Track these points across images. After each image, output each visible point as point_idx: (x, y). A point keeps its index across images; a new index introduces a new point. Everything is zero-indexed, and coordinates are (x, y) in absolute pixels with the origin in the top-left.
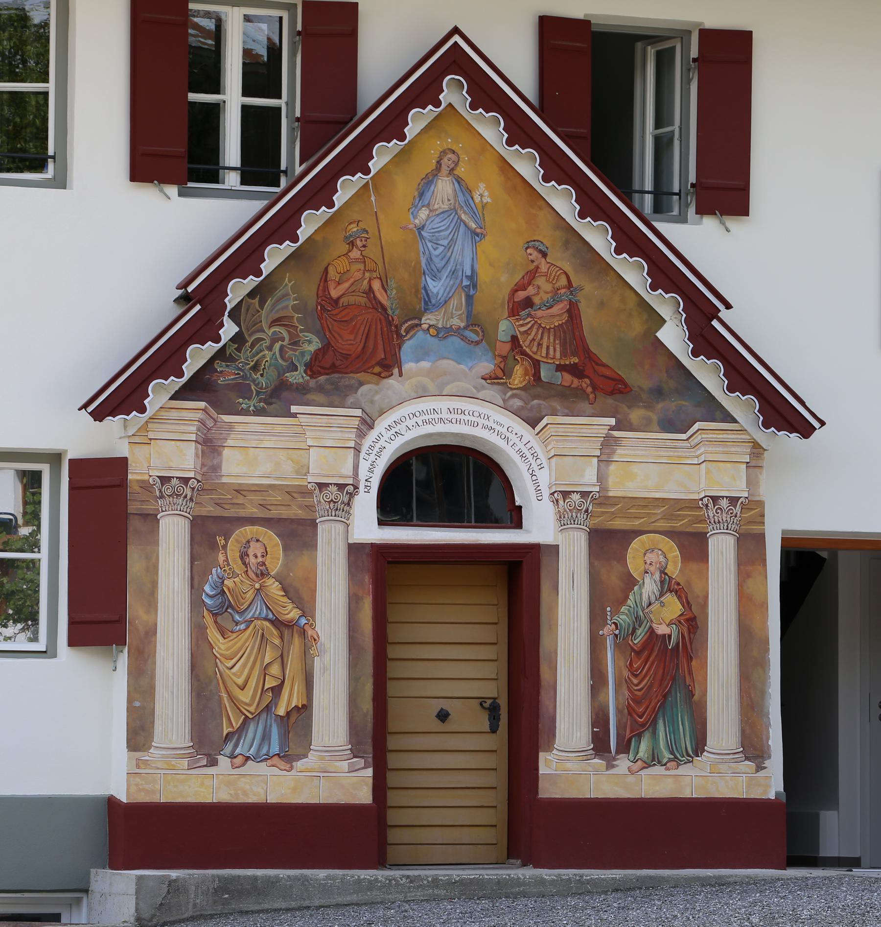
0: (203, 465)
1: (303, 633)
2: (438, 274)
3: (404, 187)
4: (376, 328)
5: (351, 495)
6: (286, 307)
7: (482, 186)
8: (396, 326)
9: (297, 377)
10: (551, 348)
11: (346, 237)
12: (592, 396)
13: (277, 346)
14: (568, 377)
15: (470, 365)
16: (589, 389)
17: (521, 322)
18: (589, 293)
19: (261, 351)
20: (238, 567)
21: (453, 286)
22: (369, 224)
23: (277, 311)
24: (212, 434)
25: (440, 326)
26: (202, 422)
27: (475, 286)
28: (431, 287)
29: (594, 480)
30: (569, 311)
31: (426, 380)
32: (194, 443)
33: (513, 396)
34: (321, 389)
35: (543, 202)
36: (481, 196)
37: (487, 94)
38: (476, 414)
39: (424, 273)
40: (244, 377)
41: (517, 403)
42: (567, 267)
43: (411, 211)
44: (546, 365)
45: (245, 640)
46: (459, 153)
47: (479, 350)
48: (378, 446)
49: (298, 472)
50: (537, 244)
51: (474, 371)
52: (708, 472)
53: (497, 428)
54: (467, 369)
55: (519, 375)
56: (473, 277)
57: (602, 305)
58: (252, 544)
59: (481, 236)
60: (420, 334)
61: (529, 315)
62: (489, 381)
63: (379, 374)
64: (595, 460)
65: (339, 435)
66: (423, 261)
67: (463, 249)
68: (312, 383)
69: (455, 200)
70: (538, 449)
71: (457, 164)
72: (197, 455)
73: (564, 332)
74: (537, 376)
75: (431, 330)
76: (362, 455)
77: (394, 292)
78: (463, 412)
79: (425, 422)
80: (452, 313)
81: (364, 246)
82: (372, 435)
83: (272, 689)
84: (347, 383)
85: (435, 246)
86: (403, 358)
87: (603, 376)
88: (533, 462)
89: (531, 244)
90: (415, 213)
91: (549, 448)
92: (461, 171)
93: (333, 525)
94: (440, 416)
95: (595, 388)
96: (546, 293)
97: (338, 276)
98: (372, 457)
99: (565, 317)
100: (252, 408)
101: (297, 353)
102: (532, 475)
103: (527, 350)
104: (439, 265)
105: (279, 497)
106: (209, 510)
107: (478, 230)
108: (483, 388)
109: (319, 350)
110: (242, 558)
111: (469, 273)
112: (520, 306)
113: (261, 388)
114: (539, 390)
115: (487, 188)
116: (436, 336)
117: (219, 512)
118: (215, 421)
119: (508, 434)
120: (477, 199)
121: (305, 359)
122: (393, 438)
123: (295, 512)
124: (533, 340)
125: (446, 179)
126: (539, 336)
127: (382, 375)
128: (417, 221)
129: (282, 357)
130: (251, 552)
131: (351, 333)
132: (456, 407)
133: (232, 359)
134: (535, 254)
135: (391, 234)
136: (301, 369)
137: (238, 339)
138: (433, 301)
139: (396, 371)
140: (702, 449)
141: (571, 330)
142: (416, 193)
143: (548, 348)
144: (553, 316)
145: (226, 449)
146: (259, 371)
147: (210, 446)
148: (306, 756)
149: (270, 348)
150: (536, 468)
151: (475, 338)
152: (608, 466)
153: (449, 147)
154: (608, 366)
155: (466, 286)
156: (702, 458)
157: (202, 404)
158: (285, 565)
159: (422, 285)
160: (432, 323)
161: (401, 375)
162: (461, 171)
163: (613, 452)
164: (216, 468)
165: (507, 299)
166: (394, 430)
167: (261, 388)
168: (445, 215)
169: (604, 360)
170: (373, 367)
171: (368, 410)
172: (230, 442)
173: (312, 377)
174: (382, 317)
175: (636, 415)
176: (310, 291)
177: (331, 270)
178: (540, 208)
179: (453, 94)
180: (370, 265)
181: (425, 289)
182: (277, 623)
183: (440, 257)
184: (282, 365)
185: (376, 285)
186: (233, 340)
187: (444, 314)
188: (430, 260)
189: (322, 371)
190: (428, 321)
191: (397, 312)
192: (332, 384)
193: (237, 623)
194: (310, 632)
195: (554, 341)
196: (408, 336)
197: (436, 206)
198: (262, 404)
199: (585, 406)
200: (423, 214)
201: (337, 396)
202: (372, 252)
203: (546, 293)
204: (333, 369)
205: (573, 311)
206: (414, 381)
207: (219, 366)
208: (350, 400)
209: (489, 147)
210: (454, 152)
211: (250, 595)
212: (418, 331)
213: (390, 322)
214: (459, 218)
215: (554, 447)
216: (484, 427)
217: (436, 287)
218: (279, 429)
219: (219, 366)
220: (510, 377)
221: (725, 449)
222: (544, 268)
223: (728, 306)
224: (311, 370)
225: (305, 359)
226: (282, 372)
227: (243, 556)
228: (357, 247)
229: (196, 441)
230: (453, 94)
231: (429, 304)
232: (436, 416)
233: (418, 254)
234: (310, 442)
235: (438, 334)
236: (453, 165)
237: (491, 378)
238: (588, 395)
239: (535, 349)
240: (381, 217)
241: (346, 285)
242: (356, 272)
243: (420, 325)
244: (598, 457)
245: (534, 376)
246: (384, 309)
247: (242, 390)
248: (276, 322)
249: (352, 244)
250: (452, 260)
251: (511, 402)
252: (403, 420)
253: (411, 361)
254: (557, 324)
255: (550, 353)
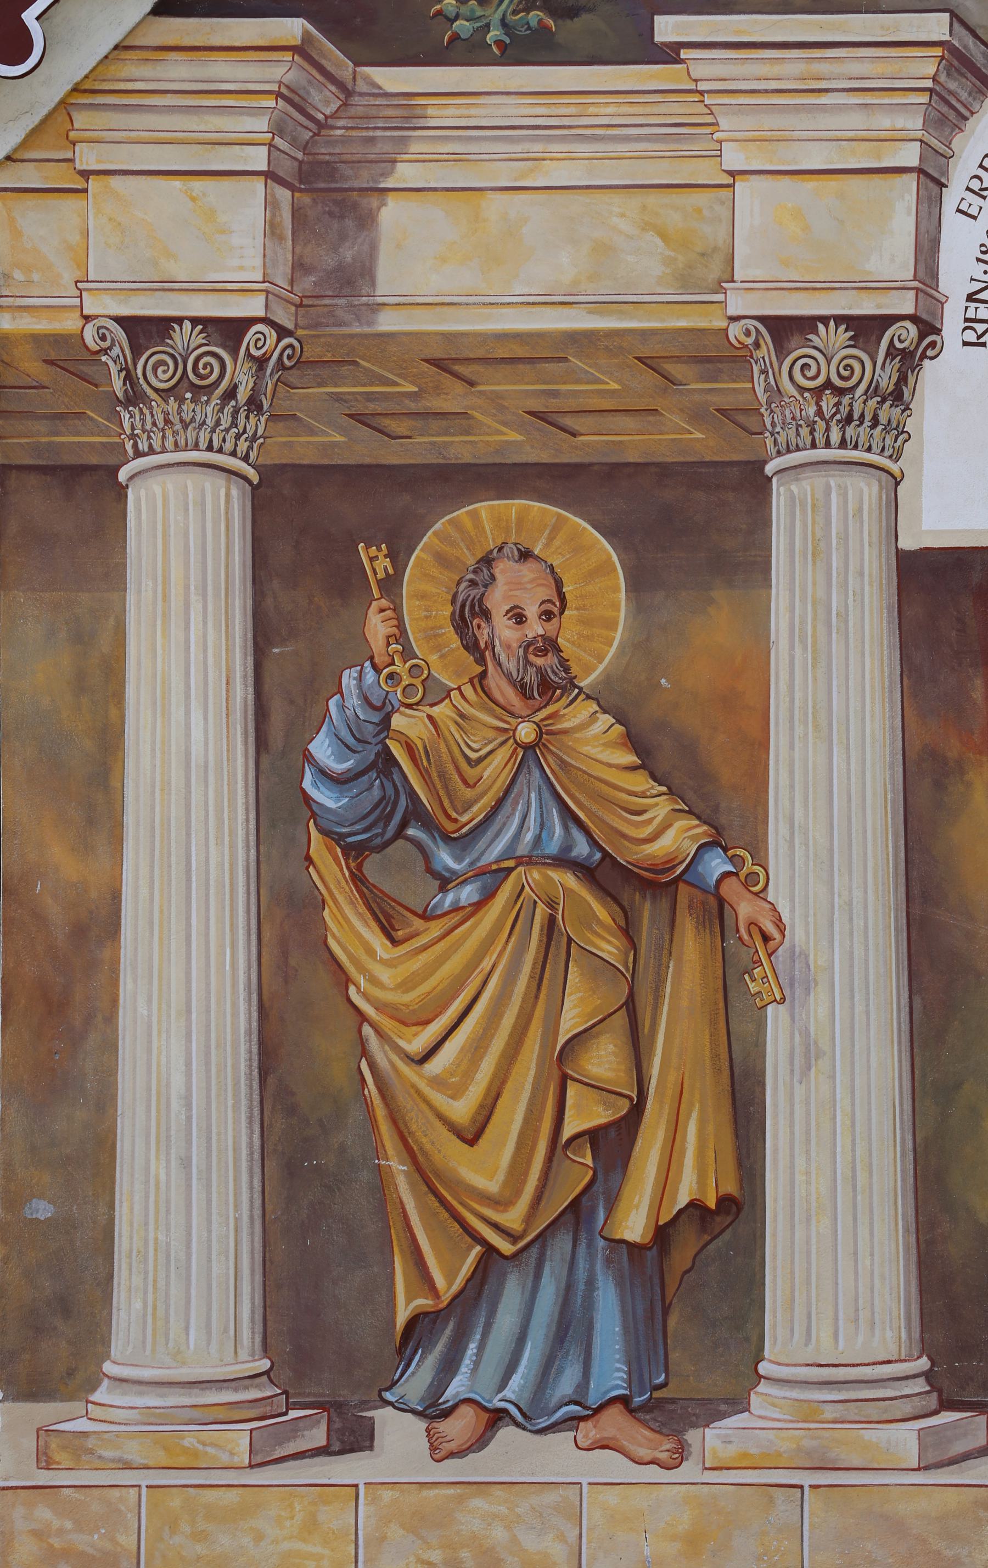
0: (299, 267)
1: (716, 912)
20: (445, 660)
24: (331, 142)
26: (290, 97)
32: (259, 184)
45: (478, 947)
49: (685, 281)
58: (504, 569)
65: (855, 122)
72: (272, 229)
76: (953, 196)
83: (594, 1136)
93: (834, 480)
100: (494, 34)
105: (608, 382)
106: (326, 440)
110: (461, 624)
117: (365, 449)
118: (347, 92)
123: (679, 436)
130: (498, 601)
145: (391, 199)
147: (325, 191)
148: (739, 1404)
157: (293, 28)
158: (640, 646)
164: (354, 279)
172: (406, 174)
182: (609, 875)
193: (445, 882)
194: (745, 909)
198: (535, 16)
211: (496, 770)
218: (607, 111)
227: (469, 616)
229: (269, 175)
234: (734, 158)
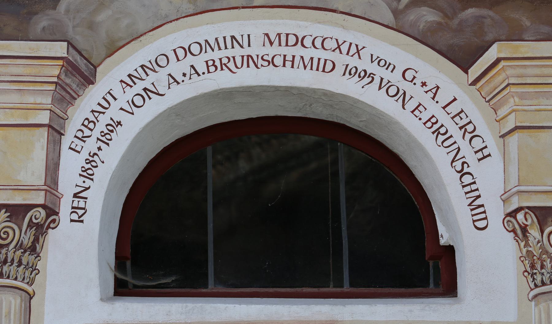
5: (40, 230)
38: (330, 44)
41: (427, 16)
48: (104, 120)
53: (380, 72)
65: (15, 98)
70: (477, 114)
76: (67, 140)
78: (300, 41)
79: (212, 66)
82: (92, 97)
88: (463, 144)
91: (502, 112)
94: (246, 51)
98: (91, 145)
102: (462, 173)
119: (404, 86)
122: (138, 101)
132: (284, 31)
166: (139, 87)
171: (81, 43)
208: (42, 22)
216: (349, 71)
232: (237, 52)
251: (412, 16)
252: (162, 61)
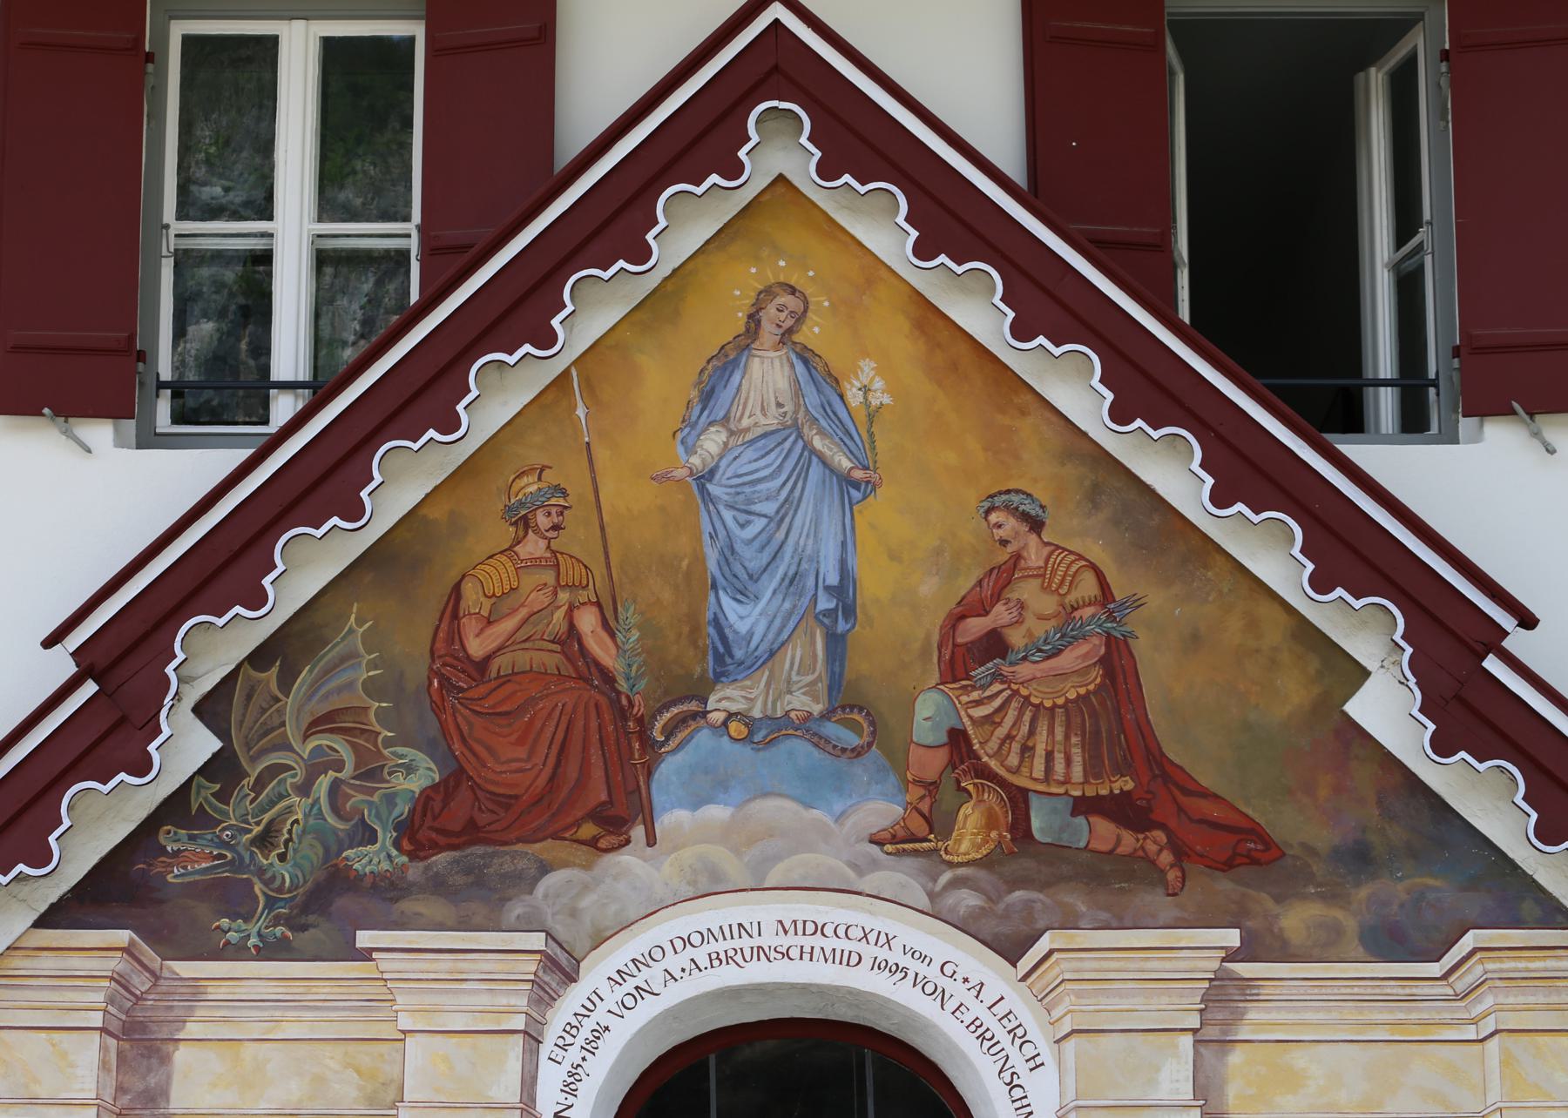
0: (120, 1089)
2: (751, 587)
3: (662, 380)
4: (586, 728)
6: (350, 685)
7: (867, 367)
8: (640, 721)
9: (375, 858)
10: (1059, 758)
11: (508, 509)
12: (1172, 875)
13: (323, 783)
14: (1105, 831)
15: (838, 807)
16: (1166, 858)
17: (975, 695)
18: (1158, 611)
19: (281, 797)
21: (790, 614)
22: (572, 475)
23: (326, 696)
24: (146, 1009)
25: (757, 713)
26: (120, 980)
27: (849, 611)
28: (732, 617)
29: (1186, 1091)
30: (1105, 662)
31: (719, 854)
32: (96, 1035)
33: (956, 883)
34: (438, 886)
35: (1029, 397)
36: (866, 390)
37: (862, 137)
38: (856, 933)
39: (714, 586)
40: (237, 865)
41: (968, 900)
42: (1097, 552)
43: (679, 436)
44: (1045, 800)
46: (808, 292)
47: (860, 771)
48: (588, 1024)
49: (371, 1100)
50: (1015, 498)
51: (849, 823)
52: (1507, 1061)
53: (914, 966)
54: (829, 820)
55: (971, 830)
56: (844, 590)
57: (1194, 641)
59: (870, 487)
60: (704, 738)
61: (997, 676)
62: (889, 848)
63: (593, 843)
64: (1187, 1041)
65: (484, 1000)
66: (712, 557)
67: (817, 522)
68: (415, 872)
69: (797, 405)
71: (800, 318)
72: (104, 1065)
73: (1094, 715)
74: (1021, 828)
75: (734, 727)
76: (546, 1049)
77: (635, 635)
78: (819, 930)
80: (789, 681)
81: (556, 527)
82: (573, 999)
84: (507, 867)
85: (742, 518)
86: (658, 798)
87: (1201, 821)
88: (1012, 1051)
89: (998, 501)
90: (690, 441)
91: (1056, 1014)
92: (812, 333)
94: (756, 942)
95: (1181, 853)
96: (1041, 618)
97: (487, 604)
98: (574, 1055)
99: (1096, 676)
100: (253, 941)
101: (376, 798)
102: (1012, 1086)
103: (993, 764)
104: (755, 564)
107: (858, 474)
108: (875, 865)
109: (434, 787)
111: (833, 579)
112: (970, 654)
113: (280, 890)
114: (1026, 865)
115: (879, 371)
116: (747, 739)
118: (156, 976)
119: (943, 982)
120: (854, 397)
121: (396, 812)
122: (629, 1002)
124: (1009, 737)
125: (772, 354)
126: (1025, 729)
127: (603, 844)
128: (695, 461)
129: (336, 810)
131: (520, 742)
132: (800, 918)
133: (204, 820)
134: (1011, 525)
135: (625, 494)
136: (386, 837)
137: (219, 769)
138: (739, 654)
139: (638, 832)
140: (1489, 1001)
141: (1113, 707)
142: (694, 393)
143: (1049, 756)
144: (1062, 676)
145: (182, 1045)
146: (275, 846)
149: (304, 789)
150: (1022, 1068)
151: (851, 739)
152: (1225, 1053)
153: (782, 279)
154: (1216, 797)
155: (827, 613)
156: (1489, 1026)
157: (123, 936)
159: (709, 615)
160: (734, 708)
161: (651, 840)
162: (812, 333)
163: (1238, 1018)
165: (936, 638)
166: (629, 986)
167: (280, 890)
168: (770, 442)
169: (1206, 780)
170: (578, 824)
171: (561, 932)
172: (192, 1029)
173: (413, 856)
174: (603, 701)
175: (1296, 919)
176: (412, 646)
177: (469, 589)
178: (1023, 413)
179: (778, 150)
180: (571, 573)
181: (717, 623)
183: (757, 544)
184: (335, 831)
185: (587, 621)
186: (206, 770)
187: (768, 685)
188: (729, 553)
189: (442, 840)
190: (725, 704)
191: (642, 685)
192: (468, 872)
195: (1067, 737)
196: (672, 744)
197: (745, 422)
198: (279, 930)
199: (1155, 899)
200: (712, 442)
201: (479, 901)
202: (578, 540)
203: (1041, 618)
204: (472, 833)
205: (1117, 663)
206: (688, 855)
207: (171, 839)
208: (516, 909)
209: (884, 273)
210: (793, 291)
212: (697, 730)
213: (622, 708)
214: (808, 448)
215: (1071, 1009)
216: (877, 965)
217: (745, 619)
218: (324, 991)
219: (171, 839)
220: (946, 835)
221: (1554, 999)
222: (1034, 555)
223: (1527, 621)
224: (412, 840)
225: (396, 812)
226: (334, 848)
228: (537, 531)
229: (103, 1030)
230: (778, 150)
231: (725, 660)
232: (746, 943)
233: (699, 540)
234: (405, 1022)
235: (751, 733)
236: (790, 322)
237: (894, 840)
238: (1163, 872)
239: (1013, 760)
240: (602, 455)
241: (508, 625)
242: (534, 589)
243: (705, 714)
244: (1195, 1031)
245: (1012, 828)
246: (608, 678)
247: (229, 895)
248: (323, 723)
249: (525, 524)
250: (788, 550)
251: (950, 900)
252: (657, 954)
253: (681, 806)
254: (1072, 695)
255: (1056, 769)
